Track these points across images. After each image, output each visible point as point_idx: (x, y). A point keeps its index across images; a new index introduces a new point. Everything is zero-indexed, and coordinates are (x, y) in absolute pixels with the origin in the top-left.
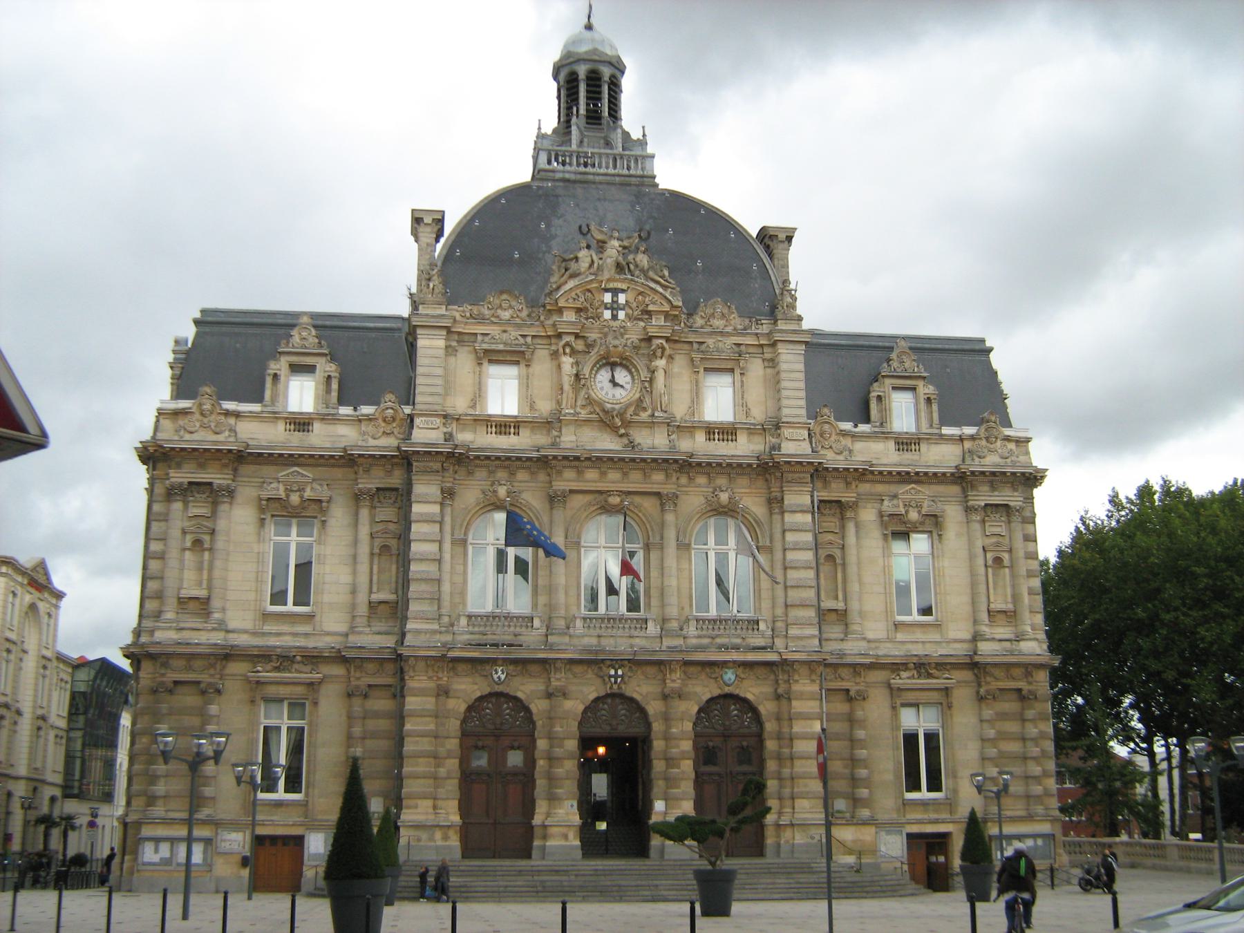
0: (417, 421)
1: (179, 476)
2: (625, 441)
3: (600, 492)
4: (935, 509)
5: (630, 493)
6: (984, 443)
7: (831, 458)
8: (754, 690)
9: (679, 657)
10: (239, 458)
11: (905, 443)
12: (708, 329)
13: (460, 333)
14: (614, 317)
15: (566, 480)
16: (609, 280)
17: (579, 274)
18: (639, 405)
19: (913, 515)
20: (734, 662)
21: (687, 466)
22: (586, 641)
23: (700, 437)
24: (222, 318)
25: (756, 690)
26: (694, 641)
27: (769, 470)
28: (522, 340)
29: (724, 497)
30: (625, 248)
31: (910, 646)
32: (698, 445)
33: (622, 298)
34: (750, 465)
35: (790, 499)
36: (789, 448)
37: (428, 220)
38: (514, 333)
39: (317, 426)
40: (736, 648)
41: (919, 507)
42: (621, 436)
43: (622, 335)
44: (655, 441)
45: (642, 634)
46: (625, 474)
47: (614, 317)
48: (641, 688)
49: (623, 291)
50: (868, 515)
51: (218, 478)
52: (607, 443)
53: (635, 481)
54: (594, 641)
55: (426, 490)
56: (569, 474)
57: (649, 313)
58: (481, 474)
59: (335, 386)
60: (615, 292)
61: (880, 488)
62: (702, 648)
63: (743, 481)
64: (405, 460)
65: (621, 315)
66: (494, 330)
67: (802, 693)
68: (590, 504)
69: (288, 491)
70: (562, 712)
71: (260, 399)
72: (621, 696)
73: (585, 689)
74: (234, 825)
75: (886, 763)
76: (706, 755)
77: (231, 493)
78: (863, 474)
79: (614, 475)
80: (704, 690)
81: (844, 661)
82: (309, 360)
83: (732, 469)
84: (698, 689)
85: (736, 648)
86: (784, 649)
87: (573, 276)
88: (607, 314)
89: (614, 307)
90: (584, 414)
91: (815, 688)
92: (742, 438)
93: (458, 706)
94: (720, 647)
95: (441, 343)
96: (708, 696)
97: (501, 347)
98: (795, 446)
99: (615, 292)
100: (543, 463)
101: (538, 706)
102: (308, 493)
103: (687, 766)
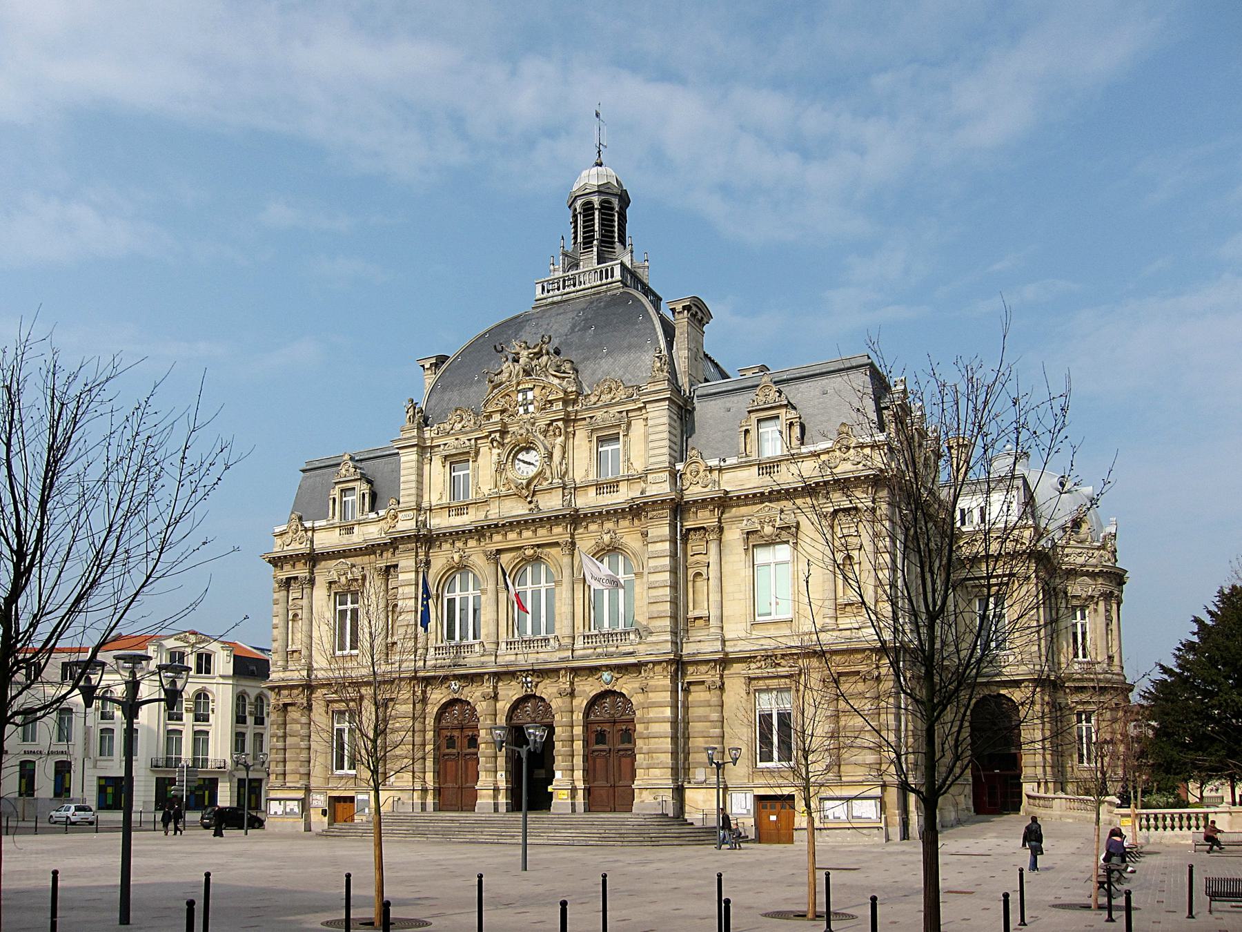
0: (400, 515)
1: (283, 575)
2: (532, 506)
3: (519, 548)
4: (790, 519)
5: (539, 546)
6: (838, 453)
7: (694, 492)
8: (626, 685)
9: (564, 665)
10: (313, 558)
11: (767, 467)
12: (600, 404)
13: (432, 447)
14: (526, 411)
15: (498, 541)
16: (518, 384)
17: (501, 384)
18: (540, 474)
19: (768, 530)
20: (607, 666)
21: (576, 519)
22: (507, 658)
23: (592, 491)
24: (318, 464)
25: (629, 686)
26: (581, 652)
27: (636, 511)
28: (467, 443)
29: (607, 538)
30: (535, 354)
31: (762, 641)
32: (587, 500)
33: (530, 395)
34: (623, 510)
35: (653, 533)
36: (652, 490)
37: (427, 366)
38: (463, 438)
39: (356, 527)
40: (610, 655)
41: (772, 521)
42: (530, 502)
43: (533, 424)
44: (551, 502)
45: (544, 649)
46: (535, 531)
47: (526, 411)
48: (547, 689)
49: (531, 389)
50: (733, 535)
51: (301, 571)
52: (518, 509)
53: (543, 535)
54: (513, 658)
55: (406, 562)
56: (497, 538)
57: (550, 402)
58: (446, 546)
59: (367, 499)
60: (524, 391)
61: (744, 510)
62: (583, 657)
63: (624, 523)
64: (394, 544)
65: (531, 408)
66: (451, 440)
67: (656, 686)
68: (515, 558)
69: (339, 576)
70: (491, 710)
71: (325, 517)
72: (534, 696)
73: (511, 693)
74: (321, 791)
75: (742, 736)
76: (595, 736)
77: (312, 582)
78: (724, 502)
79: (527, 534)
80: (589, 688)
81: (697, 658)
82: (350, 485)
83: (615, 514)
84: (587, 689)
85: (610, 655)
86: (644, 652)
87: (494, 388)
88: (521, 410)
89: (525, 404)
90: (504, 491)
91: (668, 682)
92: (623, 487)
93: (432, 710)
94: (599, 655)
95: (415, 457)
96: (594, 693)
97: (454, 451)
98: (660, 487)
99: (524, 391)
100: (480, 532)
101: (481, 707)
102: (350, 576)
103: (578, 745)
